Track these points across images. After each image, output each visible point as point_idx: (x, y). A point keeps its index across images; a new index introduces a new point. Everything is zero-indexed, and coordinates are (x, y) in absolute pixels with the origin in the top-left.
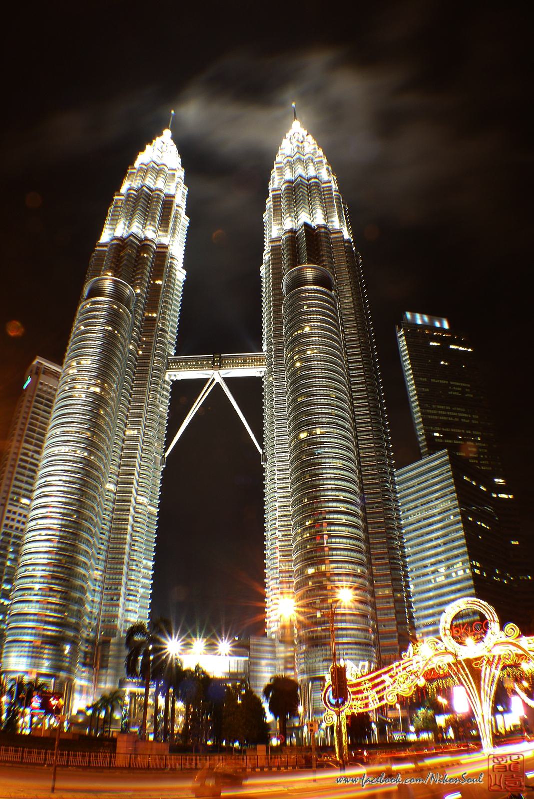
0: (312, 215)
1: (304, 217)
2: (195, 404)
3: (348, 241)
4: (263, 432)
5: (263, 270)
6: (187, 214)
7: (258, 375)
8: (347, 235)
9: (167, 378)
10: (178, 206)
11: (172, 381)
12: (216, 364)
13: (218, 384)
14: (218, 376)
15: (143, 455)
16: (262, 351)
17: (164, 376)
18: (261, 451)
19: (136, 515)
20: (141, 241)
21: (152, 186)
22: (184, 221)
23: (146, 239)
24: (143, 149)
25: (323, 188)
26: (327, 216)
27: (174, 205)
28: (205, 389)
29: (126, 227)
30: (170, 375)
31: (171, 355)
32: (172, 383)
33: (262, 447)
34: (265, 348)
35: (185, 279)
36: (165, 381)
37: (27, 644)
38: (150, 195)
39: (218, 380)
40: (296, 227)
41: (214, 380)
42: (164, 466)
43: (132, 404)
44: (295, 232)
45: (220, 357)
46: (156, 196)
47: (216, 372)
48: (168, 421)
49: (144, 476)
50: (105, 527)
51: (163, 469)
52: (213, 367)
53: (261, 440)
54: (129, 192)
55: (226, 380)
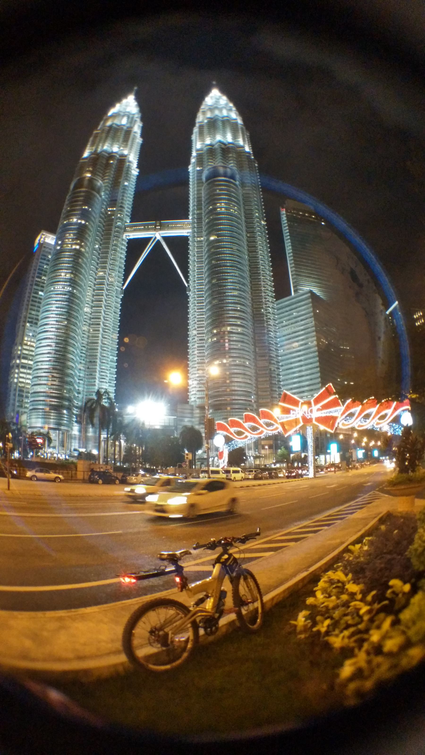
0: (224, 136)
1: (219, 138)
2: (143, 254)
3: (248, 153)
4: (188, 272)
7: (186, 234)
8: (247, 149)
9: (124, 237)
11: (127, 239)
13: (158, 241)
14: (158, 235)
15: (108, 288)
16: (188, 219)
17: (122, 236)
18: (186, 285)
19: (105, 327)
26: (235, 137)
30: (126, 236)
31: (127, 223)
32: (127, 241)
33: (188, 282)
34: (190, 217)
36: (123, 240)
37: (41, 411)
39: (159, 237)
40: (214, 143)
42: (123, 295)
43: (101, 255)
45: (160, 223)
48: (125, 266)
50: (85, 336)
51: (121, 297)
52: (155, 229)
53: (187, 277)
55: (165, 238)
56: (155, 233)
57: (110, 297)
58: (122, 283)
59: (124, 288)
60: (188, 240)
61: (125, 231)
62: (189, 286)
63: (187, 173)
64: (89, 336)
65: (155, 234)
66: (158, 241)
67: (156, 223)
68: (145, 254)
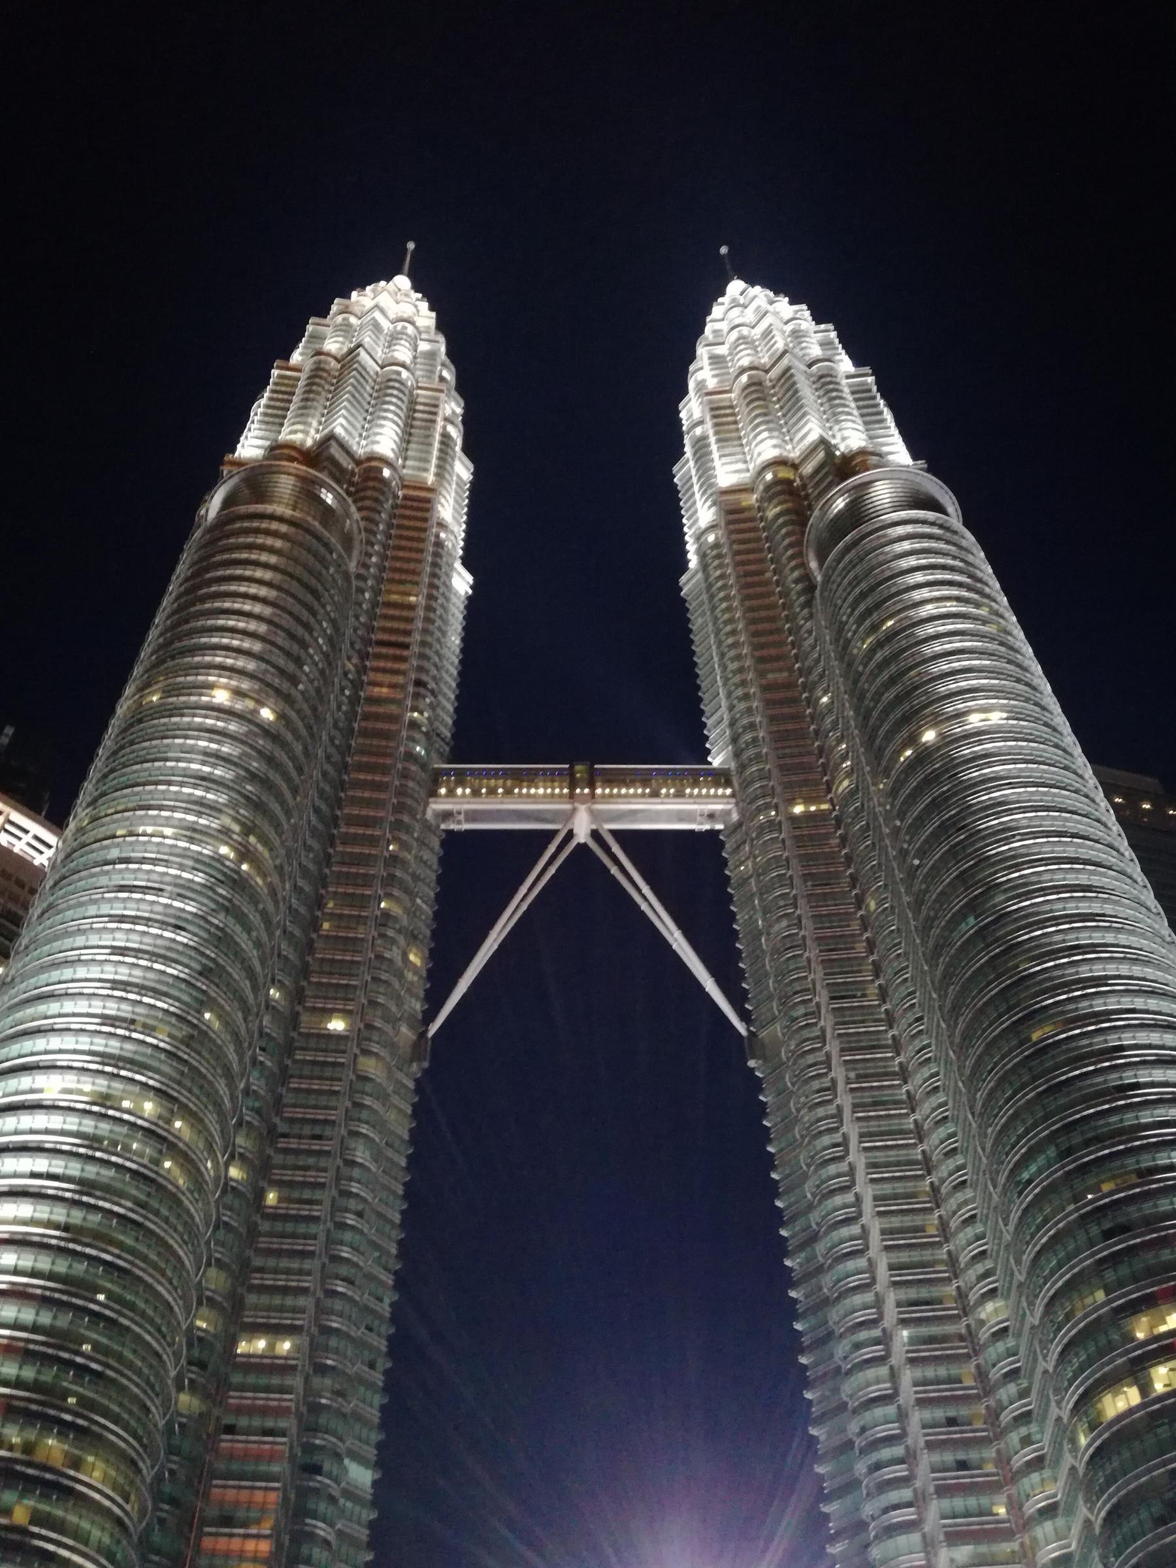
1: (812, 430)
2: (523, 890)
5: (690, 583)
12: (578, 791)
18: (741, 1028)
20: (358, 462)
21: (379, 354)
22: (463, 470)
23: (372, 457)
25: (850, 386)
28: (552, 849)
29: (312, 432)
33: (745, 1016)
35: (470, 592)
38: (377, 373)
39: (582, 835)
40: (794, 454)
42: (426, 1064)
44: (795, 466)
46: (394, 377)
53: (737, 998)
54: (322, 357)
56: (574, 810)
60: (722, 845)
63: (679, 607)
65: (570, 815)
66: (582, 847)
67: (571, 773)
68: (530, 889)
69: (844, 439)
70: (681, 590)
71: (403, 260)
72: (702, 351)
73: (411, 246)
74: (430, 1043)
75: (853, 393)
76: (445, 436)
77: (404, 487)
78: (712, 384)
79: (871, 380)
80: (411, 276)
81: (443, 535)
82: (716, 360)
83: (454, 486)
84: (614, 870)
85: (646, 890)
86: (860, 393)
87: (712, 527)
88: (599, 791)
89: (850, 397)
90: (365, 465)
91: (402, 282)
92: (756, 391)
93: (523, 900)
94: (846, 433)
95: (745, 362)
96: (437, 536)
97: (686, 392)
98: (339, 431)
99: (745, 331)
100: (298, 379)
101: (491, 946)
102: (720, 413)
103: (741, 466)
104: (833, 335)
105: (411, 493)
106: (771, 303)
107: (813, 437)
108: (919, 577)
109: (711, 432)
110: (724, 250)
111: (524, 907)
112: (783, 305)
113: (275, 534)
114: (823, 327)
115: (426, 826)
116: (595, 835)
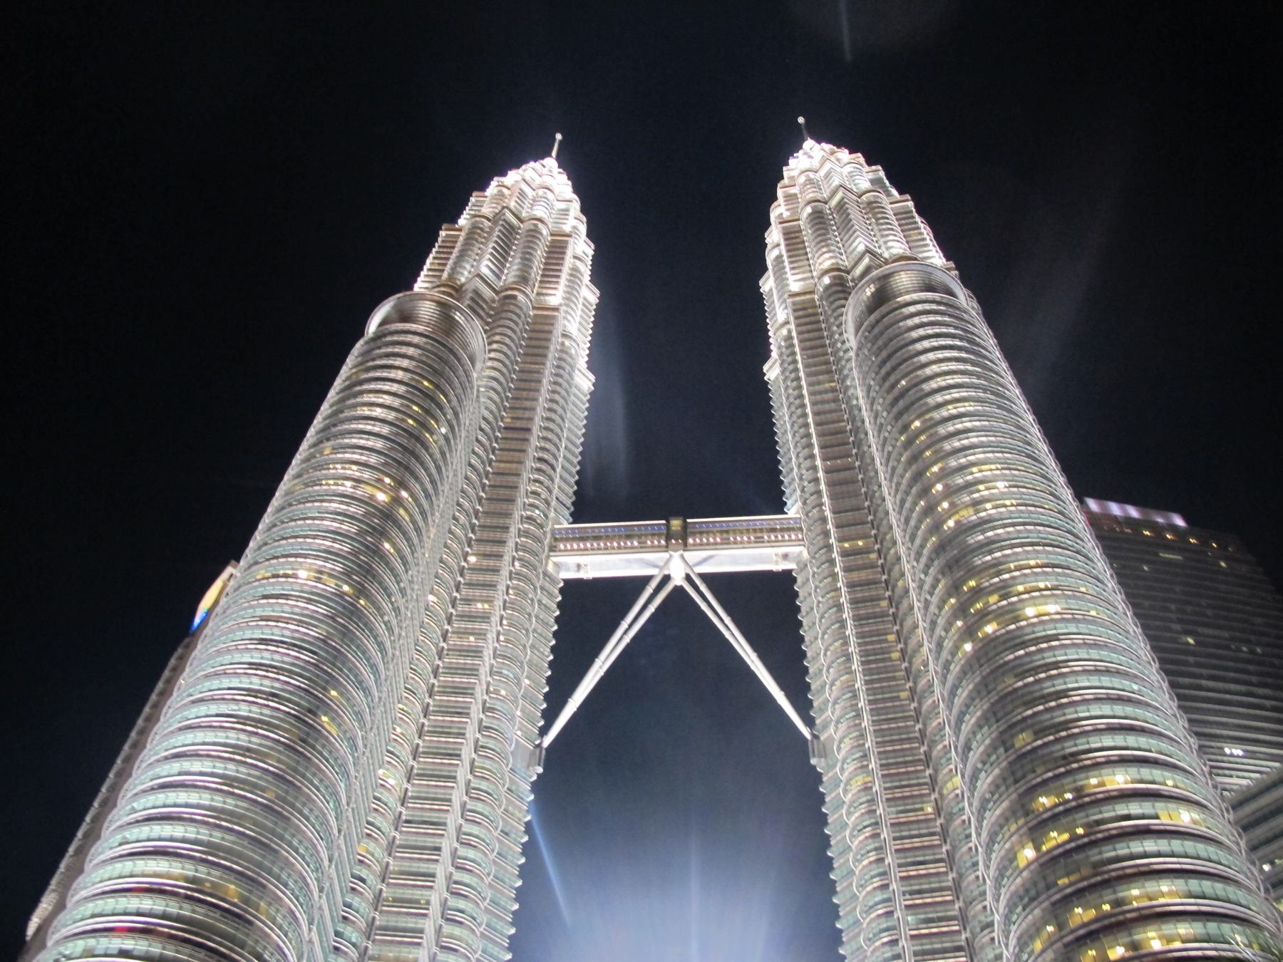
2: (624, 625)
4: (807, 687)
6: (594, 280)
9: (550, 568)
10: (575, 257)
15: (482, 741)
18: (805, 732)
22: (590, 295)
24: (504, 174)
25: (892, 209)
27: (569, 253)
28: (649, 590)
30: (556, 564)
32: (562, 584)
33: (809, 722)
39: (678, 580)
40: (846, 263)
41: (667, 579)
47: (676, 555)
49: (490, 754)
53: (804, 706)
56: (671, 556)
57: (490, 754)
58: (542, 723)
59: (548, 740)
60: (794, 580)
61: (553, 549)
62: (815, 737)
63: (762, 389)
64: (378, 896)
66: (679, 590)
67: (668, 526)
68: (631, 626)
69: (888, 248)
70: (765, 374)
71: (553, 146)
72: (780, 193)
73: (559, 137)
74: (544, 752)
75: (895, 215)
76: (575, 269)
77: (534, 308)
78: (786, 215)
79: (911, 204)
80: (558, 159)
81: (567, 343)
82: (790, 198)
83: (580, 306)
84: (703, 606)
85: (727, 620)
86: (903, 216)
87: (787, 323)
88: (691, 541)
89: (894, 218)
90: (503, 294)
91: (551, 162)
92: (818, 218)
93: (626, 632)
94: (890, 244)
95: (811, 196)
96: (563, 344)
97: (770, 224)
98: (485, 271)
99: (811, 175)
100: (459, 236)
101: (597, 671)
102: (792, 237)
103: (809, 275)
104: (882, 174)
105: (540, 312)
106: (833, 153)
107: (861, 248)
108: (926, 344)
109: (784, 252)
110: (801, 120)
111: (627, 639)
112: (844, 154)
113: (409, 344)
114: (874, 168)
115: (545, 574)
116: (688, 578)
